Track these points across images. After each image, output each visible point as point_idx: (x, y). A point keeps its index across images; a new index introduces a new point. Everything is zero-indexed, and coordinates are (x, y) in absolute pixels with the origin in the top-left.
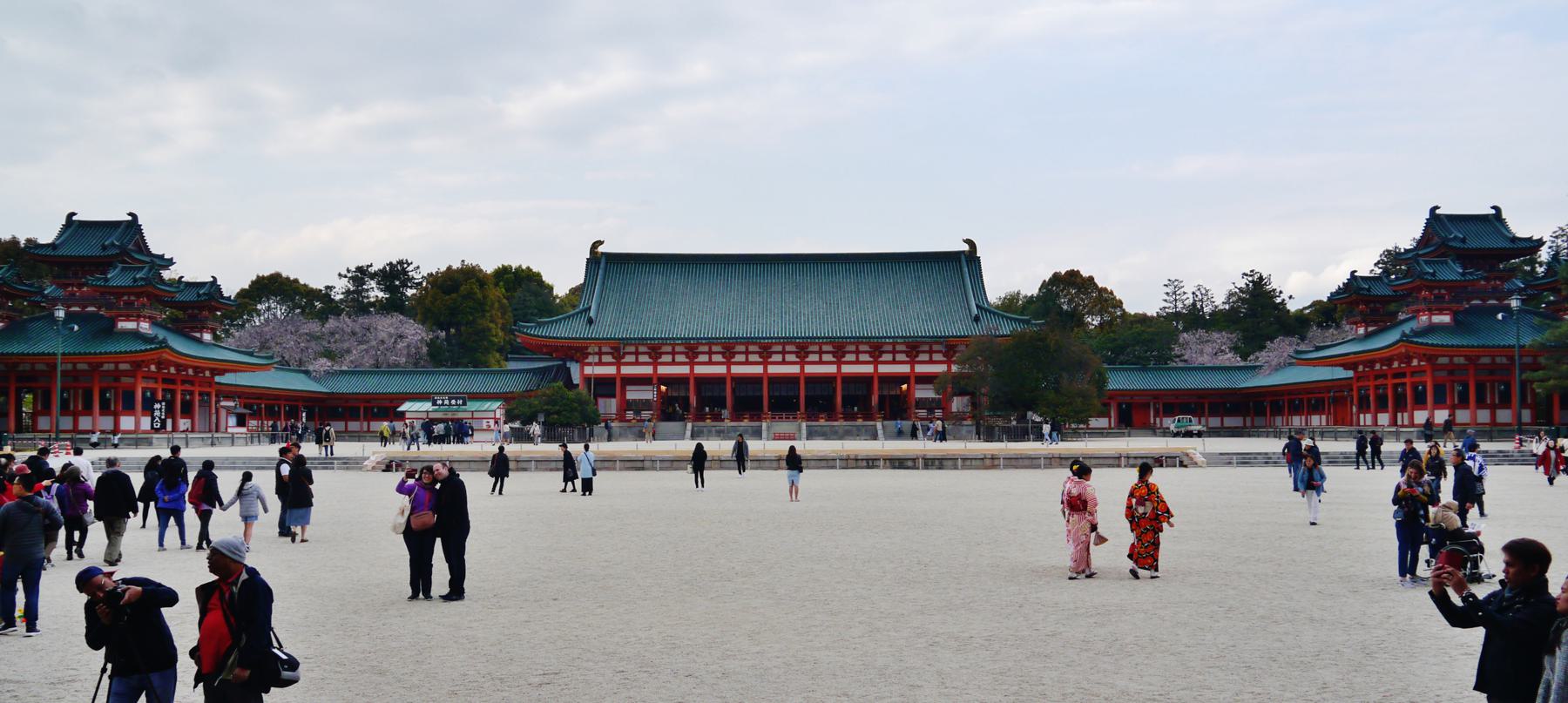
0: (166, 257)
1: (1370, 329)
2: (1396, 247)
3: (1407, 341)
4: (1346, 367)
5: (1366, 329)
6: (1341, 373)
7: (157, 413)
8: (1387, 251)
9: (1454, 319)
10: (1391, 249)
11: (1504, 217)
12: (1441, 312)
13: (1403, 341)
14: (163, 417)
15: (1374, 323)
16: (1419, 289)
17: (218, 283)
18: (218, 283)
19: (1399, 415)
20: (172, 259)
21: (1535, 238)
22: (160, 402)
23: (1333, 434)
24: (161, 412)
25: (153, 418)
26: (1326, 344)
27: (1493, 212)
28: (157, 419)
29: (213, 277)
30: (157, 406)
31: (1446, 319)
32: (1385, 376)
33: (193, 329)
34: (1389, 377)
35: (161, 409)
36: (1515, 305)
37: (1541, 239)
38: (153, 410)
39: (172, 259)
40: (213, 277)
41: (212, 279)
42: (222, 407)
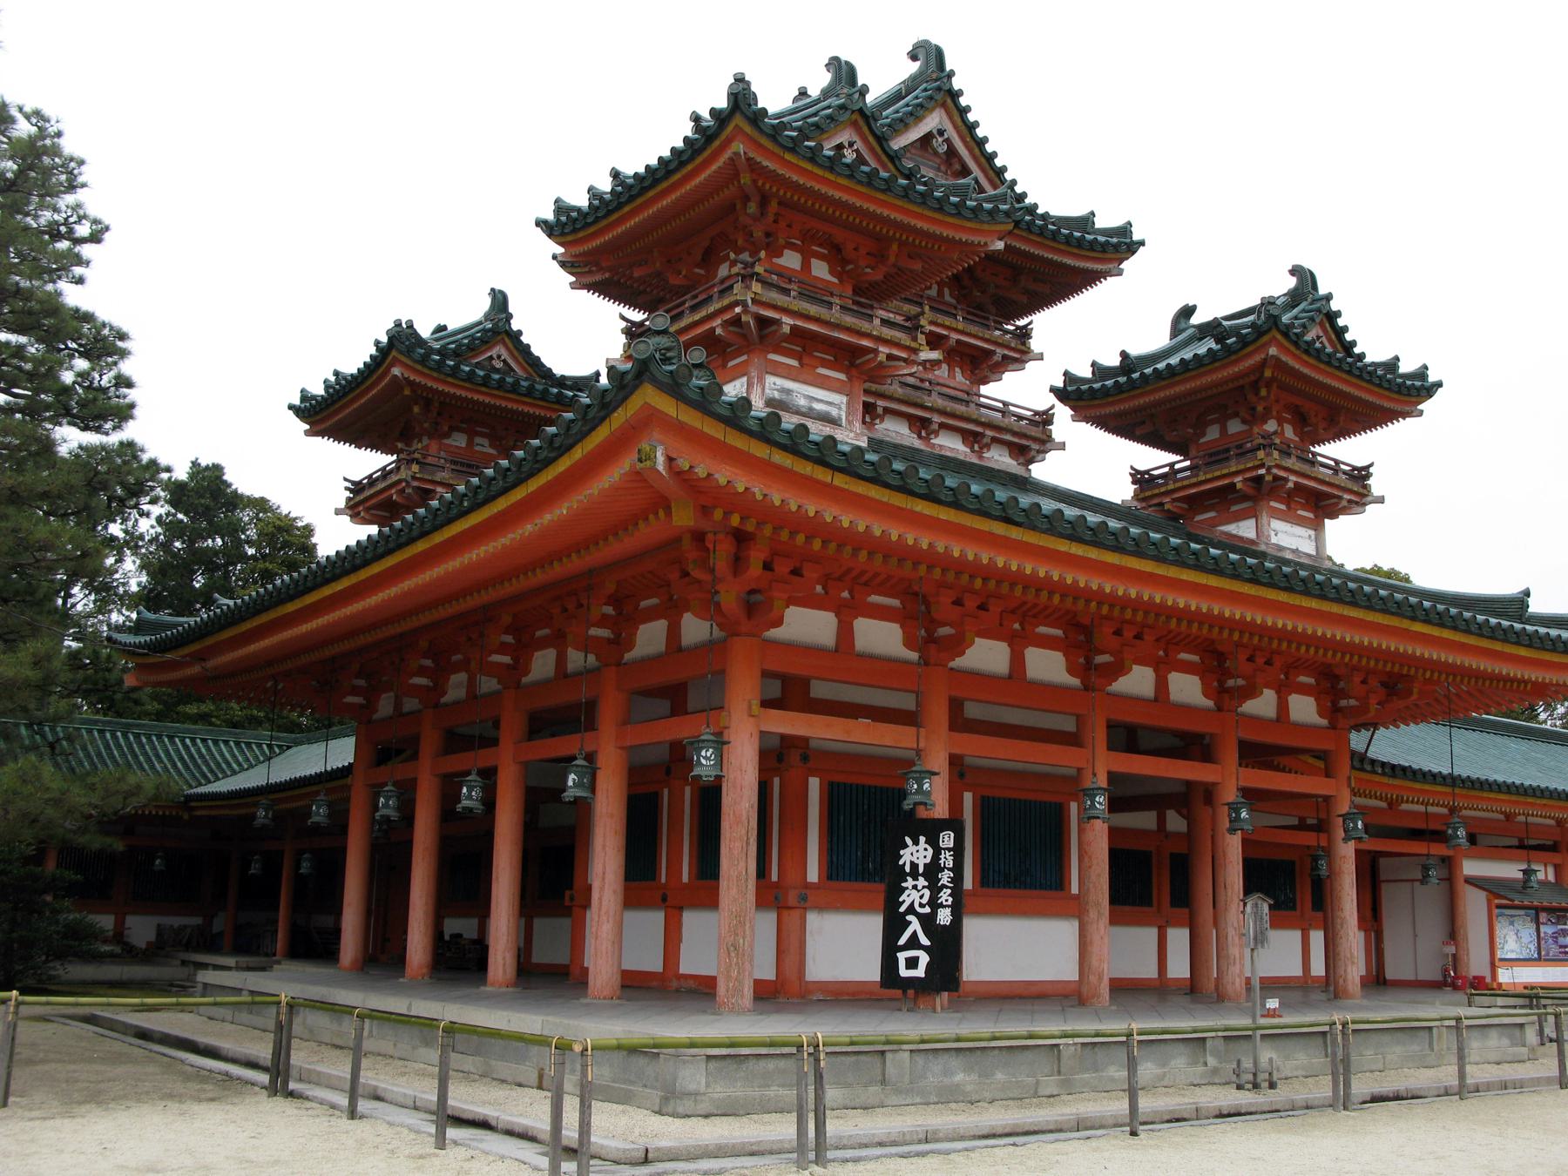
0: (1100, 223)
7: (914, 895)
14: (944, 917)
17: (1322, 291)
18: (1322, 291)
20: (1125, 230)
22: (931, 831)
24: (935, 888)
25: (893, 925)
28: (915, 925)
29: (1296, 271)
30: (916, 853)
33: (1225, 500)
35: (932, 871)
38: (895, 878)
39: (1125, 230)
40: (1296, 271)
41: (1292, 282)
42: (1472, 881)
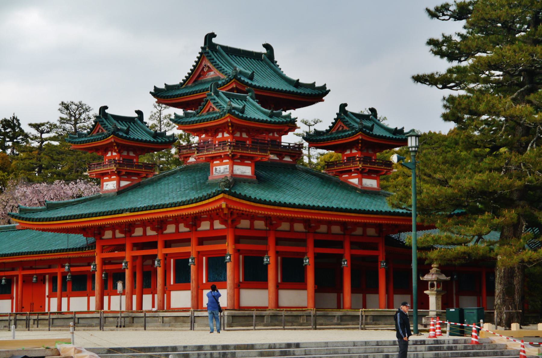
1: (124, 183)
2: (14, 117)
3: (229, 193)
4: (84, 231)
5: (118, 184)
6: (79, 240)
8: (5, 120)
9: (255, 172)
10: (8, 118)
11: (275, 59)
12: (242, 160)
13: (224, 192)
15: (128, 175)
16: (106, 149)
19: (106, 298)
21: (317, 85)
23: (47, 322)
26: (62, 202)
27: (264, 51)
31: (246, 170)
32: (121, 248)
34: (160, 245)
36: (414, 145)
37: (324, 87)
